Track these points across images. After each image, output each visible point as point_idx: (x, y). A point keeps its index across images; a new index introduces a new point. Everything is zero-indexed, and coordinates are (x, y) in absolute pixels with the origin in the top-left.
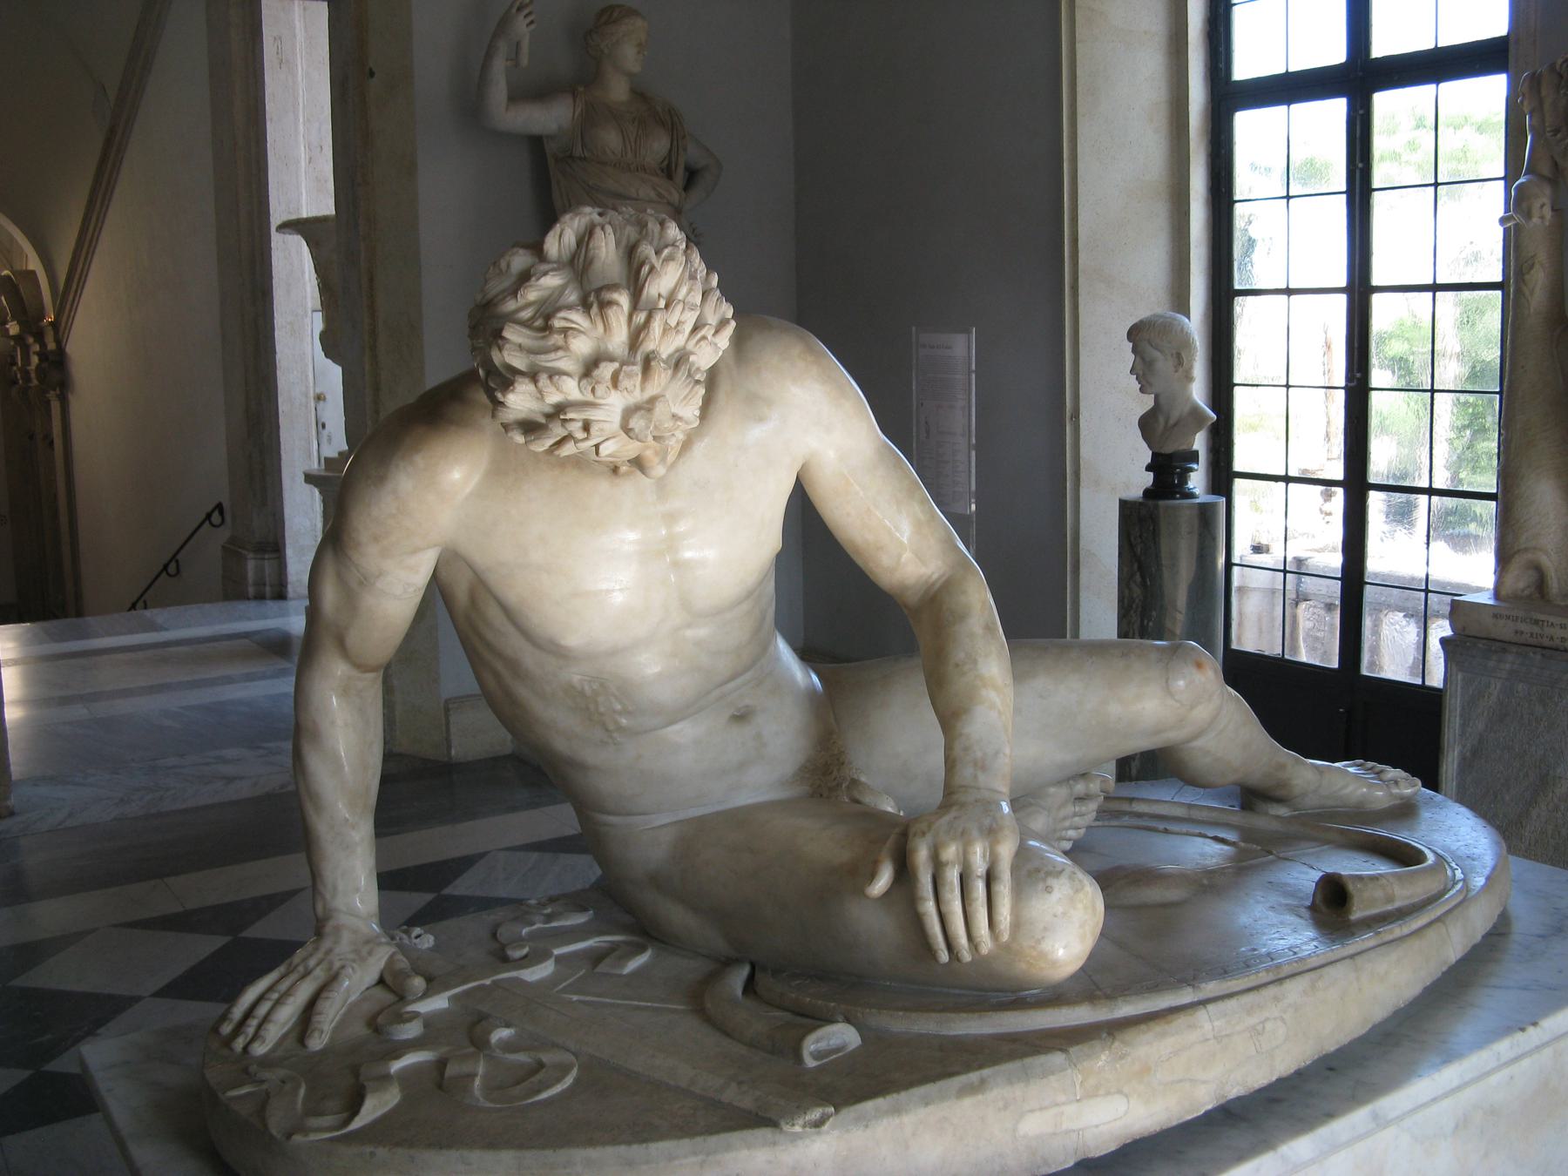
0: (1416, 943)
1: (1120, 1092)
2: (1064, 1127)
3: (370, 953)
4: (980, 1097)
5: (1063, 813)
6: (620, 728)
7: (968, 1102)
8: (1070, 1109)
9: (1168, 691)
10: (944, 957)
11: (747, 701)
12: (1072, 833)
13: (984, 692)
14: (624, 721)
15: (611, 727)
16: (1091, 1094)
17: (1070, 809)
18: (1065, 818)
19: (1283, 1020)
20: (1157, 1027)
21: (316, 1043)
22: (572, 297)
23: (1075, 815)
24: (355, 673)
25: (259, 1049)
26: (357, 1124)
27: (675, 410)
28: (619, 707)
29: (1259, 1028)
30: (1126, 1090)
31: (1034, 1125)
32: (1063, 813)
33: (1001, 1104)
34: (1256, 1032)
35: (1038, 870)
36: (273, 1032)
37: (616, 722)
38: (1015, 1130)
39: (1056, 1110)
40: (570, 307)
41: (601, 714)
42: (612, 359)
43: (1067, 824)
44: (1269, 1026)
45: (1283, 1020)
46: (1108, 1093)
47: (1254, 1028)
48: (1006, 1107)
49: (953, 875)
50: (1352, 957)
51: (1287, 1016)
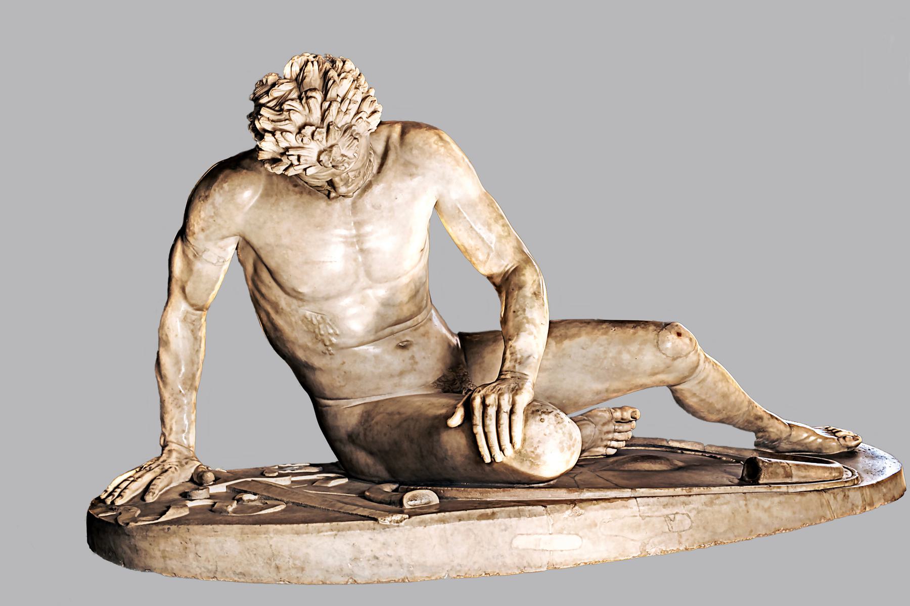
0: (798, 498)
1: (577, 535)
2: (541, 548)
3: (186, 463)
4: (491, 521)
5: (606, 429)
6: (332, 345)
7: (484, 522)
9: (657, 346)
10: (488, 460)
11: (408, 338)
12: (614, 444)
13: (527, 325)
14: (334, 340)
15: (328, 343)
18: (608, 432)
19: (688, 516)
20: (603, 504)
21: (150, 499)
22: (294, 95)
23: (615, 431)
24: (190, 309)
25: (119, 502)
26: (163, 519)
27: (343, 152)
28: (331, 331)
29: (672, 517)
30: (581, 534)
31: (521, 542)
32: (606, 429)
33: (503, 527)
35: (538, 411)
36: (128, 496)
37: (330, 341)
38: (511, 543)
40: (292, 100)
41: (321, 335)
42: (311, 125)
43: (610, 436)
44: (678, 517)
45: (688, 516)
47: (667, 516)
48: (506, 530)
49: (492, 411)
51: (692, 515)
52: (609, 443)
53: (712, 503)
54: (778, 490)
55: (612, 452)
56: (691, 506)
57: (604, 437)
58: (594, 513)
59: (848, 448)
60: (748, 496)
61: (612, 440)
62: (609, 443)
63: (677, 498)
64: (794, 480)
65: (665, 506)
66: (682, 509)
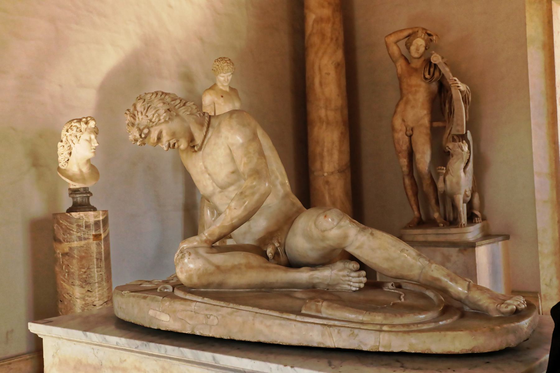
5: (341, 273)
8: (158, 313)
12: (351, 283)
16: (163, 312)
17: (345, 273)
18: (344, 276)
23: (348, 276)
29: (209, 316)
31: (151, 313)
34: (207, 317)
39: (155, 311)
44: (212, 317)
46: (166, 313)
47: (207, 315)
48: (148, 305)
50: (256, 313)
51: (219, 317)
52: (349, 283)
53: (231, 314)
54: (287, 317)
55: (354, 289)
56: (220, 313)
57: (344, 279)
58: (178, 305)
59: (503, 313)
60: (258, 315)
61: (349, 281)
62: (349, 283)
63: (215, 307)
64: (324, 315)
65: (207, 310)
66: (214, 313)
